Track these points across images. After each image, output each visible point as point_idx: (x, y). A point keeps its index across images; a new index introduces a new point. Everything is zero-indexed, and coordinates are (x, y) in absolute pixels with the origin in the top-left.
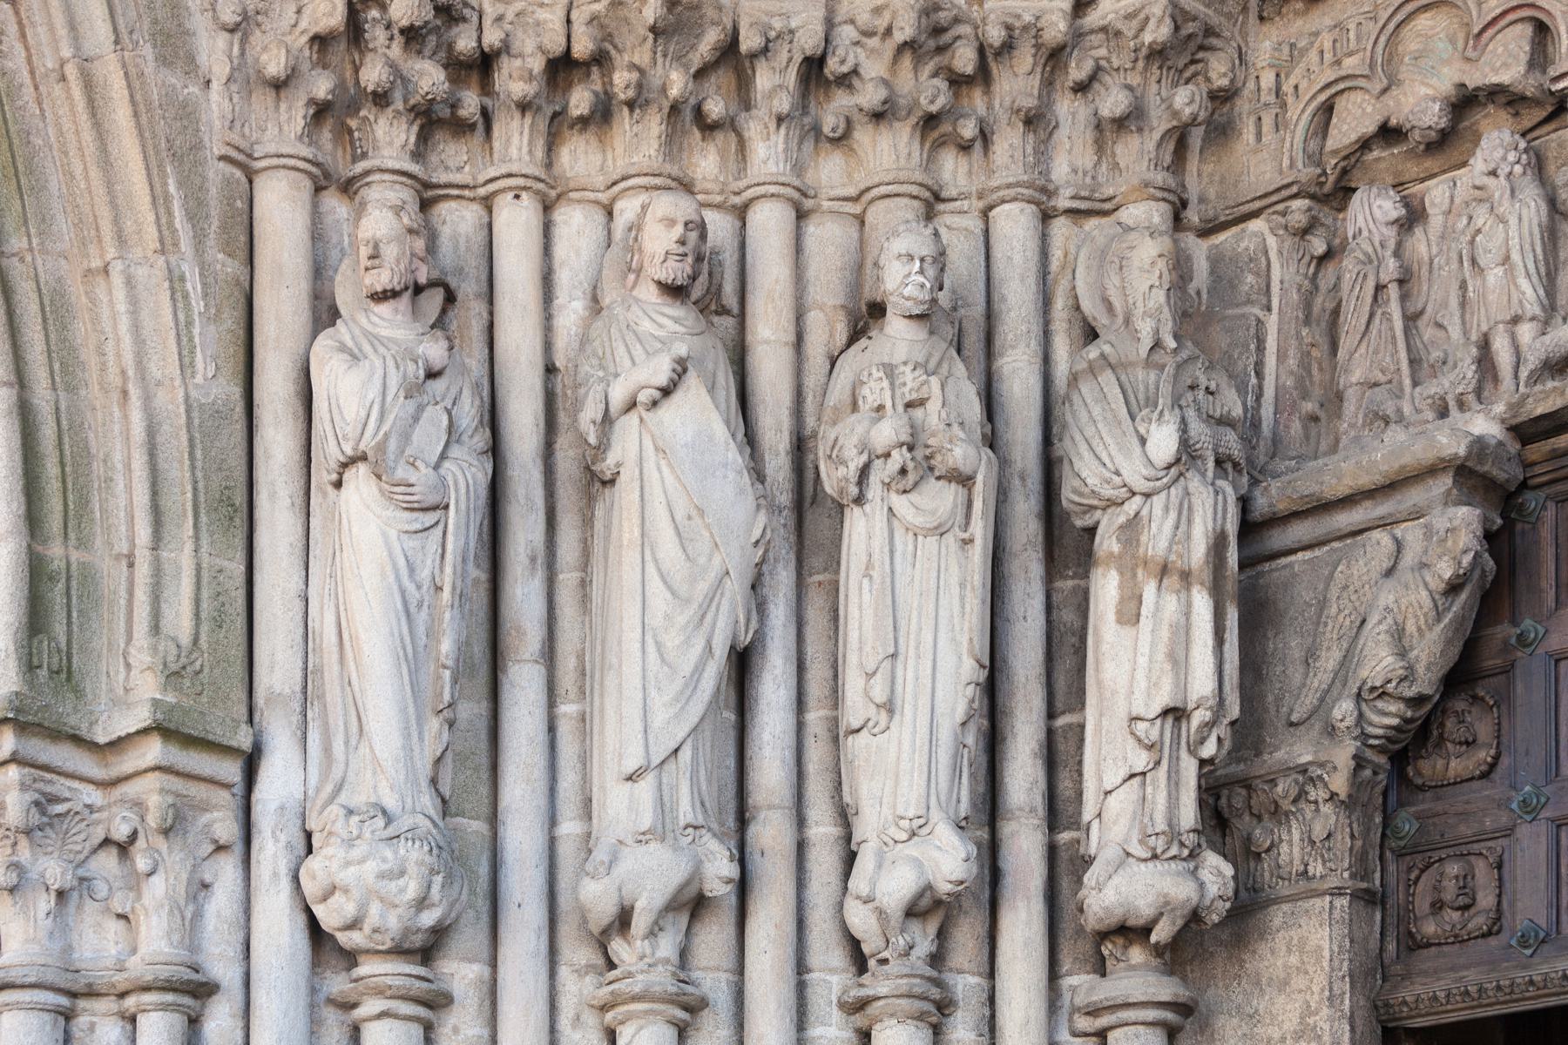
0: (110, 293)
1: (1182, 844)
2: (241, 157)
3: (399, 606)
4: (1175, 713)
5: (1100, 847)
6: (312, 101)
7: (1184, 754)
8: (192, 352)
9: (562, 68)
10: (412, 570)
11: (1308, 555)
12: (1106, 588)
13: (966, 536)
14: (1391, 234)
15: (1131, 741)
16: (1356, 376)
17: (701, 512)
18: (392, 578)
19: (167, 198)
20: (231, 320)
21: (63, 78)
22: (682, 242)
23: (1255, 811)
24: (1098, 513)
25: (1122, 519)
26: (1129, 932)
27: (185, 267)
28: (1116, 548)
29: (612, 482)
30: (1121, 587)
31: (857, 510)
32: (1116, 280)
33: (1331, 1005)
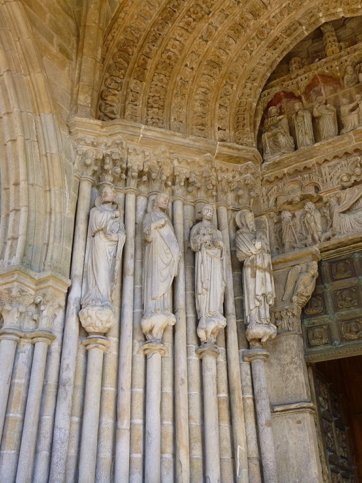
0: (50, 194)
1: (267, 321)
2: (79, 177)
3: (106, 259)
4: (264, 295)
6: (94, 170)
7: (266, 303)
8: (66, 207)
9: (141, 174)
10: (110, 253)
11: (282, 270)
13: (221, 259)
14: (290, 218)
15: (256, 300)
16: (287, 240)
17: (169, 249)
18: (105, 253)
19: (64, 180)
20: (74, 204)
21: (46, 156)
22: (165, 201)
23: (276, 318)
25: (250, 259)
27: (66, 192)
28: (249, 264)
29: (150, 242)
30: (251, 271)
31: (200, 252)
33: (298, 357)
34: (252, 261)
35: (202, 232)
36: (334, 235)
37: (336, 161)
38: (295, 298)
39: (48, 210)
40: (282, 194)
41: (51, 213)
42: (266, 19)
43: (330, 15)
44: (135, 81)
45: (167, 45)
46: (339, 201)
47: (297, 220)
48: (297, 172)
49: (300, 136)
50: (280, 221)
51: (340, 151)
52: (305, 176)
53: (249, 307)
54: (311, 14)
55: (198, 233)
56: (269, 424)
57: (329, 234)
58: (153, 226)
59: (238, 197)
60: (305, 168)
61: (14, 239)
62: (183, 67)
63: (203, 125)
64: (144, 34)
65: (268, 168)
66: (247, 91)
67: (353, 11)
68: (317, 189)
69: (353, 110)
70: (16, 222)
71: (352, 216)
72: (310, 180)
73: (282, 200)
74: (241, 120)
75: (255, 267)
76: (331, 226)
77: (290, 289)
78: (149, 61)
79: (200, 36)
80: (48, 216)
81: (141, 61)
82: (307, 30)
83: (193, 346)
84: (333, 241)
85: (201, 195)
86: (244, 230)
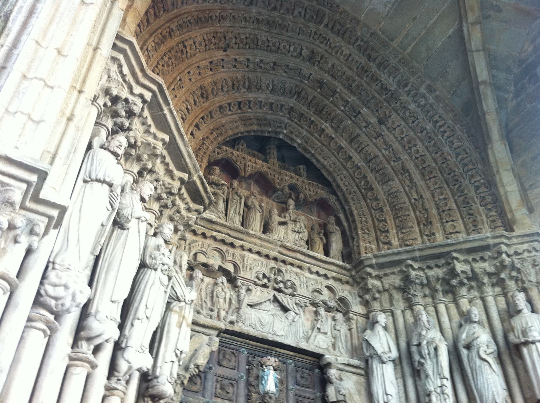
5: (161, 375)
24: (173, 301)
28: (178, 310)
29: (124, 229)
31: (153, 271)
32: (179, 258)
34: (181, 308)
36: (237, 322)
37: (256, 257)
38: (192, 366)
39: (68, 113)
40: (204, 253)
41: (69, 119)
43: (290, 137)
48: (223, 241)
49: (232, 212)
51: (265, 251)
52: (230, 252)
53: (164, 358)
57: (233, 318)
62: (186, 72)
67: (305, 149)
71: (257, 314)
72: (233, 258)
73: (201, 258)
79: (210, 60)
80: (65, 120)
82: (269, 132)
84: (236, 328)
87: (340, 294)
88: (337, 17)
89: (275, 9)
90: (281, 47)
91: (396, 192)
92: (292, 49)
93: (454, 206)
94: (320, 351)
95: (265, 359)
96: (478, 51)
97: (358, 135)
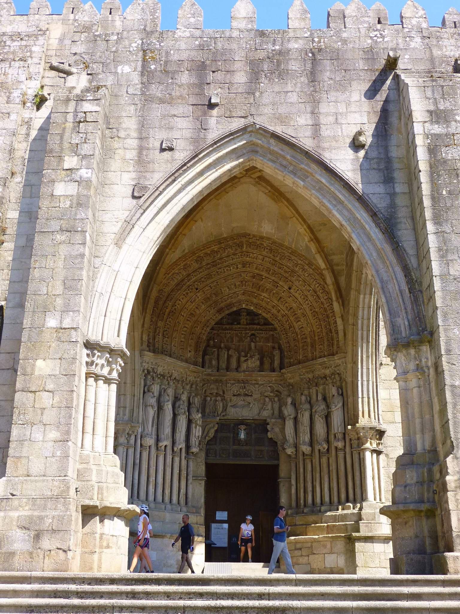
12: (194, 425)
26: (193, 453)
34: (196, 421)
35: (181, 407)
38: (207, 438)
41: (134, 396)
42: (221, 298)
44: (160, 322)
45: (175, 303)
46: (231, 400)
47: (212, 402)
50: (205, 400)
54: (240, 302)
55: (179, 407)
56: (191, 484)
57: (224, 414)
58: (166, 404)
59: (191, 387)
60: (221, 380)
61: (125, 407)
63: (183, 349)
64: (166, 294)
65: (205, 375)
66: (203, 332)
68: (224, 393)
69: (245, 361)
70: (125, 400)
74: (198, 347)
75: (197, 424)
76: (226, 410)
77: (206, 433)
78: (167, 310)
81: (164, 311)
83: (171, 453)
84: (225, 418)
85: (179, 385)
86: (194, 406)
87: (276, 389)
88: (251, 241)
89: (214, 257)
90: (225, 270)
91: (302, 327)
92: (231, 268)
93: (324, 334)
94: (264, 419)
95: (239, 426)
96: (316, 254)
97: (281, 298)
